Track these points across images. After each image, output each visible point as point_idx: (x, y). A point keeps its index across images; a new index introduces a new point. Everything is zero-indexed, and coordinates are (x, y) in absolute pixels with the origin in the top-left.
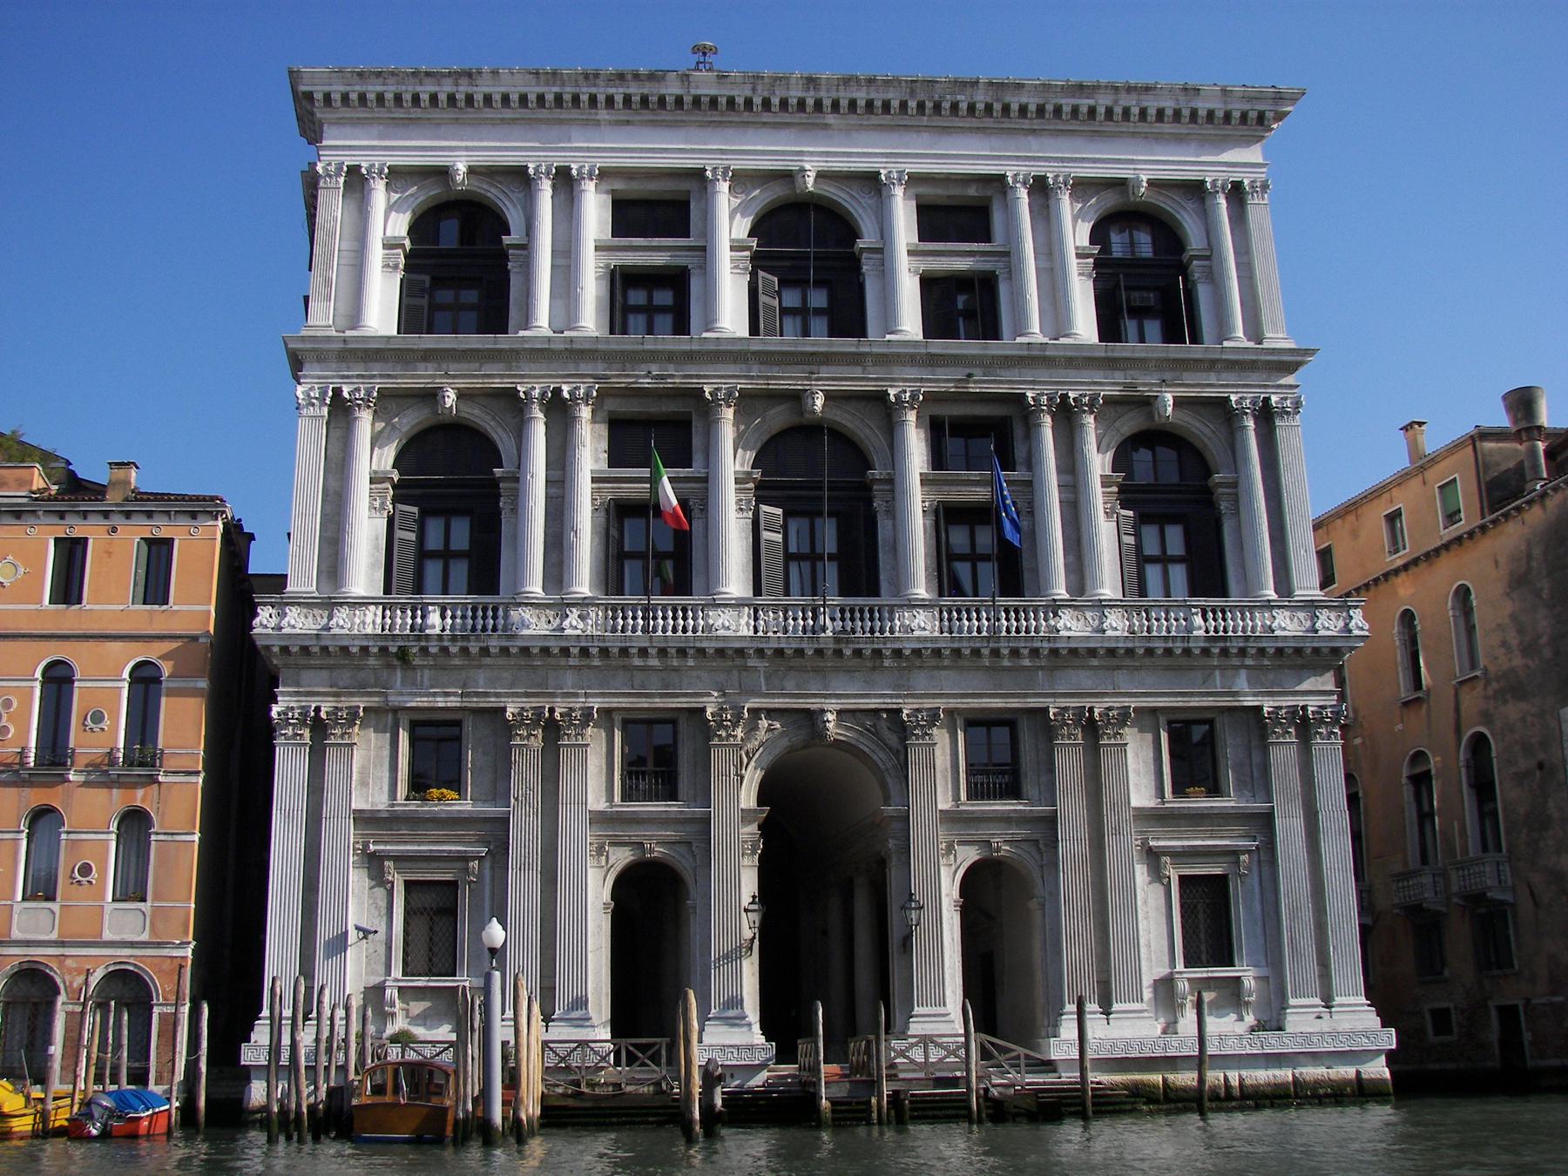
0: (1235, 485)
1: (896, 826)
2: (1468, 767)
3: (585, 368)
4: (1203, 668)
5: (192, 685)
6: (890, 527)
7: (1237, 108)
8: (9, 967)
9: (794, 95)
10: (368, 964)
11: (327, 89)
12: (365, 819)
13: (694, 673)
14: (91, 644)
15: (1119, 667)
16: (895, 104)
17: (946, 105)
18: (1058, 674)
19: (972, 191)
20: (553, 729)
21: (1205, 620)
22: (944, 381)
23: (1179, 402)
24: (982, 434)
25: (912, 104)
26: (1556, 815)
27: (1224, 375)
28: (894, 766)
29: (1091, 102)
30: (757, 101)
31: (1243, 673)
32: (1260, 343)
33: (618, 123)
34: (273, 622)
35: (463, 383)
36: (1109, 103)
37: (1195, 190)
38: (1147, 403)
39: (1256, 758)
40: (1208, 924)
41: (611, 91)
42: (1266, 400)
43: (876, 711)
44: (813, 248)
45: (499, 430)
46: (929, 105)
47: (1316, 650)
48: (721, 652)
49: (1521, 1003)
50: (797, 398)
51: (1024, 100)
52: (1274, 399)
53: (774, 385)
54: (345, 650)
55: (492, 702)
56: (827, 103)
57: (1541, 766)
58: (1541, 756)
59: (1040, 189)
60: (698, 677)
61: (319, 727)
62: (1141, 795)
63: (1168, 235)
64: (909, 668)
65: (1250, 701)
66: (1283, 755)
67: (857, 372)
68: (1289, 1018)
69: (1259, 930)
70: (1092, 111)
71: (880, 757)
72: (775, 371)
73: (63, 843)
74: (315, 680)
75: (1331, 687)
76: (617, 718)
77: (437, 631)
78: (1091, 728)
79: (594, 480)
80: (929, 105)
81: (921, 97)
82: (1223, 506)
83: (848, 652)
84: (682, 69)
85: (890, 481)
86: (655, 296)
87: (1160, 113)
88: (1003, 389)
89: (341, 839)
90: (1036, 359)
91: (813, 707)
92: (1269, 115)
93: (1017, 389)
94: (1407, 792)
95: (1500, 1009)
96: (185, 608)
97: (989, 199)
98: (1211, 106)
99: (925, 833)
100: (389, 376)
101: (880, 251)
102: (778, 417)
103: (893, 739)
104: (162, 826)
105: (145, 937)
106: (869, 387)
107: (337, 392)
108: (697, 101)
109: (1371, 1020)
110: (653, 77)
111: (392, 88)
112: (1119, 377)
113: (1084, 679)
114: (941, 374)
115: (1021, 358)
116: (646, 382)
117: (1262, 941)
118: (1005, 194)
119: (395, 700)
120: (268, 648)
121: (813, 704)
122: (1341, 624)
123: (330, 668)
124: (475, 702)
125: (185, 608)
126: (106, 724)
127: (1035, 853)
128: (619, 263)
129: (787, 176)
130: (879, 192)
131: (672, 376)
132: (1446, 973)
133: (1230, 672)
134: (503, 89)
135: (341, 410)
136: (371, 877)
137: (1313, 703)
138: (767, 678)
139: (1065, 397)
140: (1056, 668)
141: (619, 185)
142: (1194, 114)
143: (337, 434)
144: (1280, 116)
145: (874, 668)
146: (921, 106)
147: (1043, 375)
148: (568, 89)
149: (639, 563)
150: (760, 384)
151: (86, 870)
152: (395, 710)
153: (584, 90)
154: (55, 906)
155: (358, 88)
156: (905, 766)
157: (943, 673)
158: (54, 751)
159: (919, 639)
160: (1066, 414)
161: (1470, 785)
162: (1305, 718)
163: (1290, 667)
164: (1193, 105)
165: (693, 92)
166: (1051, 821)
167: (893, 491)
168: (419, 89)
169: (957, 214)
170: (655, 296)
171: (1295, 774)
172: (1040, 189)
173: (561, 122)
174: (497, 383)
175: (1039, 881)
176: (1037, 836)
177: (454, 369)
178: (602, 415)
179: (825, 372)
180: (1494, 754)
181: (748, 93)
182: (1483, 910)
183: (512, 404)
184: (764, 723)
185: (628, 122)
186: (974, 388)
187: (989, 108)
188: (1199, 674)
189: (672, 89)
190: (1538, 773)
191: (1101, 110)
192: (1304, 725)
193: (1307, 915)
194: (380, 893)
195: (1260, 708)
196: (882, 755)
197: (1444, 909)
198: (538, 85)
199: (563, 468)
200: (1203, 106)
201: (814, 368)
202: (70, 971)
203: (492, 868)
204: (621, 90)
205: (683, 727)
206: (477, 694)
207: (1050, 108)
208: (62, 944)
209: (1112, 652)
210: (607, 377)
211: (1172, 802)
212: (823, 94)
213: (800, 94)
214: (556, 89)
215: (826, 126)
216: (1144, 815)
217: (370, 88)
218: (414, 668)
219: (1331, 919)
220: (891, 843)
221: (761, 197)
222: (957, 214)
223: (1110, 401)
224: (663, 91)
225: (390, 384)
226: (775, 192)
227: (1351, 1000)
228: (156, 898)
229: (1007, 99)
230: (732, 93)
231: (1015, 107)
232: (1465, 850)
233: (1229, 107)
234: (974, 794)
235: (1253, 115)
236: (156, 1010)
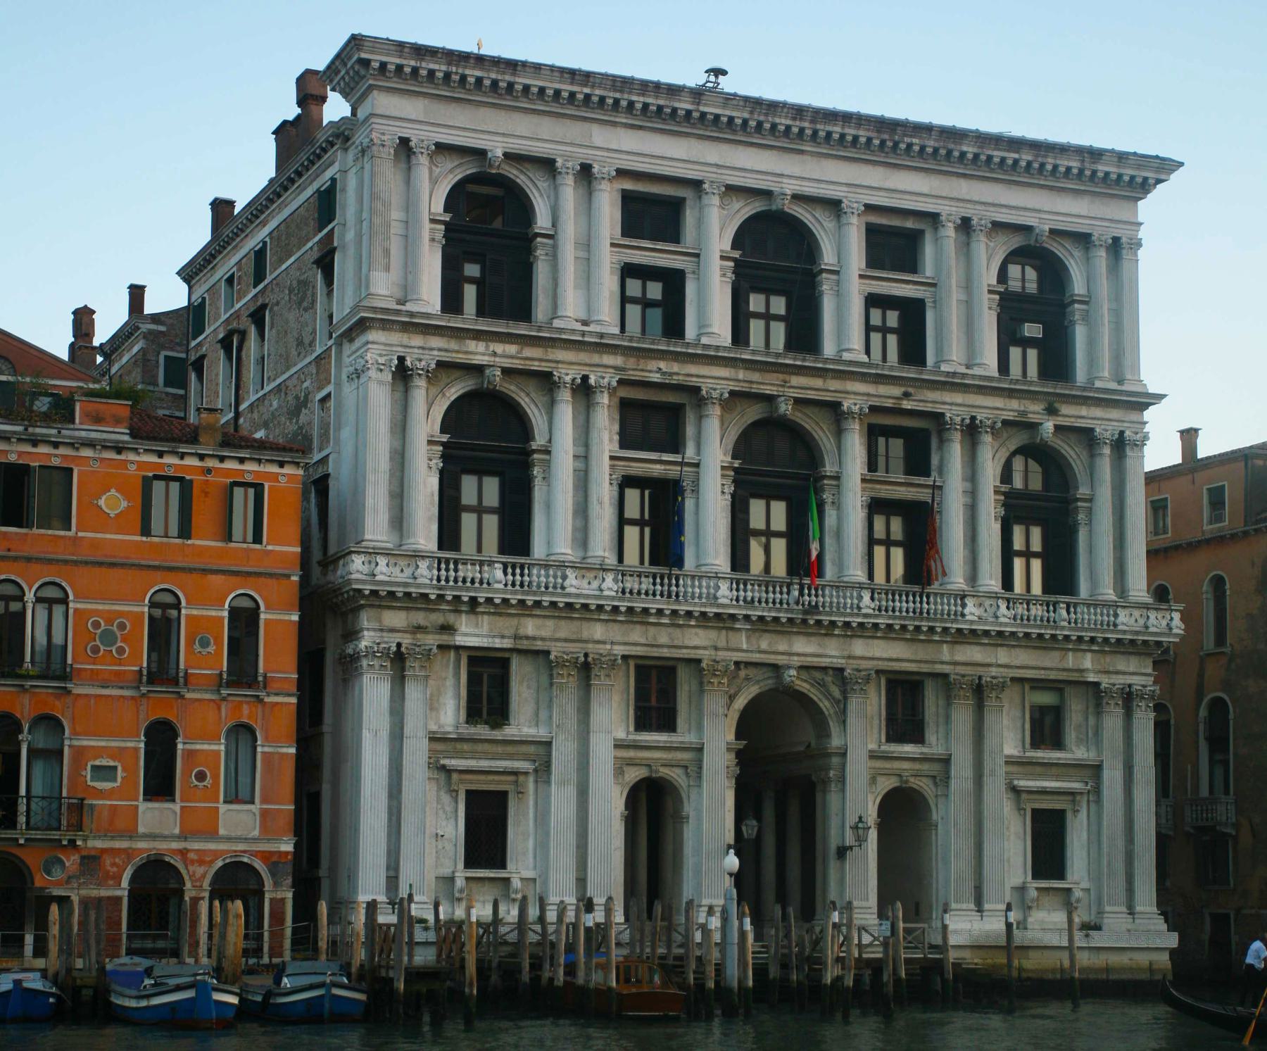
0: (1090, 500)
1: (835, 760)
3: (609, 359)
4: (1063, 649)
5: (287, 618)
6: (834, 517)
7: (1128, 172)
8: (137, 861)
9: (783, 121)
10: (437, 858)
11: (384, 59)
12: (434, 739)
13: (694, 630)
15: (1002, 645)
16: (863, 140)
17: (903, 146)
18: (958, 647)
19: (909, 224)
20: (585, 669)
21: (1068, 613)
22: (888, 394)
23: (1058, 428)
24: (911, 440)
25: (876, 142)
27: (1093, 408)
28: (836, 713)
29: (1016, 156)
30: (753, 124)
31: (1089, 655)
32: (1120, 382)
33: (632, 127)
34: (365, 569)
35: (507, 363)
36: (1030, 158)
37: (1083, 240)
38: (1033, 427)
39: (1092, 721)
41: (634, 98)
42: (1122, 433)
43: (824, 669)
44: (777, 253)
45: (533, 406)
46: (890, 144)
47: (1145, 642)
48: (717, 615)
50: (770, 399)
51: (965, 148)
52: (1127, 433)
53: (755, 389)
54: (425, 596)
55: (539, 645)
56: (809, 132)
59: (965, 225)
60: (696, 634)
61: (398, 659)
62: (1011, 748)
63: (1053, 272)
64: (851, 637)
65: (1092, 678)
66: (1113, 721)
67: (818, 383)
68: (1106, 921)
69: (1085, 854)
70: (1016, 162)
71: (825, 705)
72: (756, 376)
73: (179, 753)
74: (395, 619)
75: (1150, 670)
76: (632, 663)
77: (501, 586)
78: (979, 691)
79: (612, 458)
80: (890, 144)
81: (886, 136)
82: (1081, 516)
83: (812, 622)
84: (691, 83)
85: (837, 478)
86: (661, 295)
87: (1069, 169)
88: (929, 408)
89: (417, 753)
90: (952, 384)
91: (780, 663)
92: (1151, 181)
93: (939, 409)
96: (278, 548)
97: (922, 232)
98: (1107, 169)
99: (858, 767)
100: (446, 350)
101: (837, 273)
102: (754, 413)
103: (836, 692)
104: (266, 739)
105: (256, 833)
106: (828, 397)
107: (401, 359)
108: (703, 115)
110: (674, 91)
111: (444, 68)
112: (1015, 404)
113: (974, 653)
114: (883, 390)
115: (945, 383)
116: (656, 377)
117: (1086, 862)
118: (936, 229)
119: (460, 640)
120: (359, 591)
121: (781, 660)
122: (1164, 623)
123: (407, 609)
124: (525, 644)
125: (278, 548)
126: (211, 649)
127: (932, 786)
128: (628, 260)
129: (767, 194)
130: (839, 217)
131: (678, 374)
133: (1080, 654)
134: (541, 84)
135: (403, 374)
136: (439, 789)
137: (1136, 680)
138: (748, 638)
139: (973, 418)
140: (956, 643)
141: (629, 185)
142: (1094, 172)
143: (398, 395)
144: (1159, 181)
145: (826, 635)
146: (883, 143)
147: (958, 398)
148: (598, 92)
149: (636, 529)
150: (744, 387)
151: (201, 776)
152: (458, 648)
153: (611, 94)
154: (177, 807)
155: (413, 63)
156: (844, 711)
157: (876, 642)
158: (162, 671)
159: (866, 616)
160: (972, 430)
162: (1130, 694)
163: (1123, 653)
164: (1094, 167)
165: (702, 109)
166: (946, 761)
167: (838, 486)
168: (467, 72)
169: (895, 243)
170: (661, 295)
171: (1119, 735)
172: (965, 225)
173: (585, 119)
174: (536, 366)
175: (933, 807)
177: (499, 348)
178: (616, 400)
179: (796, 380)
181: (746, 115)
183: (546, 382)
184: (742, 673)
185: (640, 128)
186: (907, 405)
187: (936, 150)
188: (1056, 654)
189: (684, 105)
191: (1023, 164)
192: (1128, 698)
193: (1120, 843)
194: (446, 799)
195: (1097, 684)
196: (827, 703)
197: (1171, 833)
198: (572, 84)
199: (587, 446)
200: (1102, 168)
201: (787, 377)
202: (193, 862)
203: (536, 782)
204: (641, 99)
205: (683, 675)
206: (527, 638)
207: (983, 158)
208: (183, 837)
209: (1000, 634)
210: (623, 369)
211: (1032, 754)
212: (806, 124)
213: (789, 122)
214: (587, 90)
215: (802, 152)
216: (1010, 762)
217: (424, 65)
218: (476, 613)
219: (1138, 848)
220: (832, 773)
221: (743, 210)
222: (895, 243)
223: (1006, 423)
224: (677, 105)
225: (446, 357)
226: (757, 206)
227: (1148, 909)
228: (264, 801)
229: (951, 146)
230: (734, 114)
231: (956, 154)
232: (1196, 788)
233: (1122, 171)
234: (889, 739)
235: (1139, 180)
236: (267, 896)
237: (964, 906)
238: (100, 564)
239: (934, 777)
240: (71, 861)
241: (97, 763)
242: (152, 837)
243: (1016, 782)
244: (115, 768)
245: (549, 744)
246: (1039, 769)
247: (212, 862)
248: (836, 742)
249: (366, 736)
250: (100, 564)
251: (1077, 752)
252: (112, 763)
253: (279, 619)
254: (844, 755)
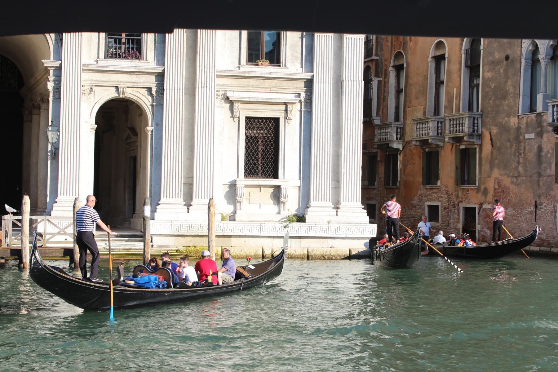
2: (467, 54)
26: (511, 90)
40: (262, 151)
49: (477, 207)
57: (507, 58)
58: (509, 52)
94: (432, 66)
95: (467, 209)
109: (363, 216)
132: (439, 184)
161: (466, 66)
180: (482, 47)
182: (463, 147)
190: (505, 62)
219: (344, 152)
237: (173, 200)
239: (150, 90)
243: (229, 94)
246: (253, 82)
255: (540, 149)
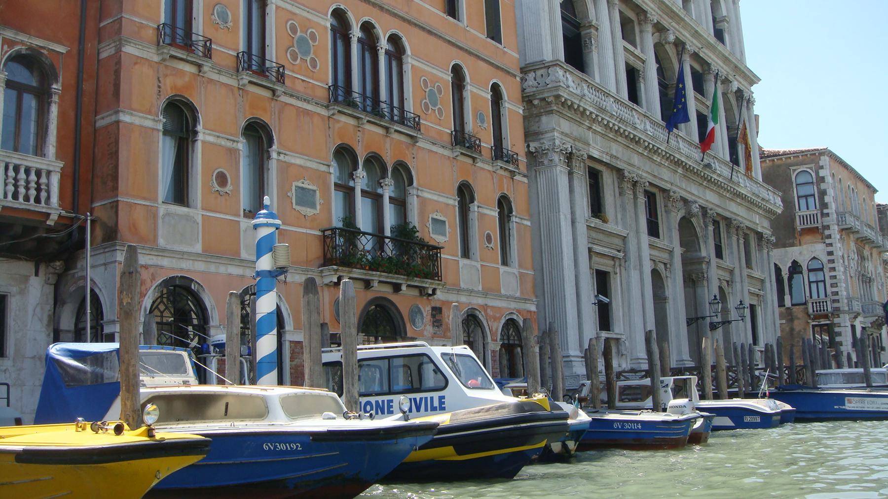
14: (473, 58)
71: (698, 230)
74: (565, 126)
124: (614, 163)
166: (731, 272)
176: (728, 279)
208: (485, 294)
238: (423, 29)
239: (728, 282)
240: (426, 310)
241: (435, 217)
242: (470, 292)
244: (444, 222)
245: (624, 239)
247: (500, 318)
248: (704, 253)
249: (562, 217)
250: (423, 29)
251: (757, 274)
252: (442, 218)
253: (512, 108)
254: (708, 263)
255: (792, 329)
